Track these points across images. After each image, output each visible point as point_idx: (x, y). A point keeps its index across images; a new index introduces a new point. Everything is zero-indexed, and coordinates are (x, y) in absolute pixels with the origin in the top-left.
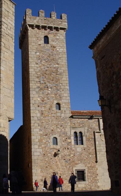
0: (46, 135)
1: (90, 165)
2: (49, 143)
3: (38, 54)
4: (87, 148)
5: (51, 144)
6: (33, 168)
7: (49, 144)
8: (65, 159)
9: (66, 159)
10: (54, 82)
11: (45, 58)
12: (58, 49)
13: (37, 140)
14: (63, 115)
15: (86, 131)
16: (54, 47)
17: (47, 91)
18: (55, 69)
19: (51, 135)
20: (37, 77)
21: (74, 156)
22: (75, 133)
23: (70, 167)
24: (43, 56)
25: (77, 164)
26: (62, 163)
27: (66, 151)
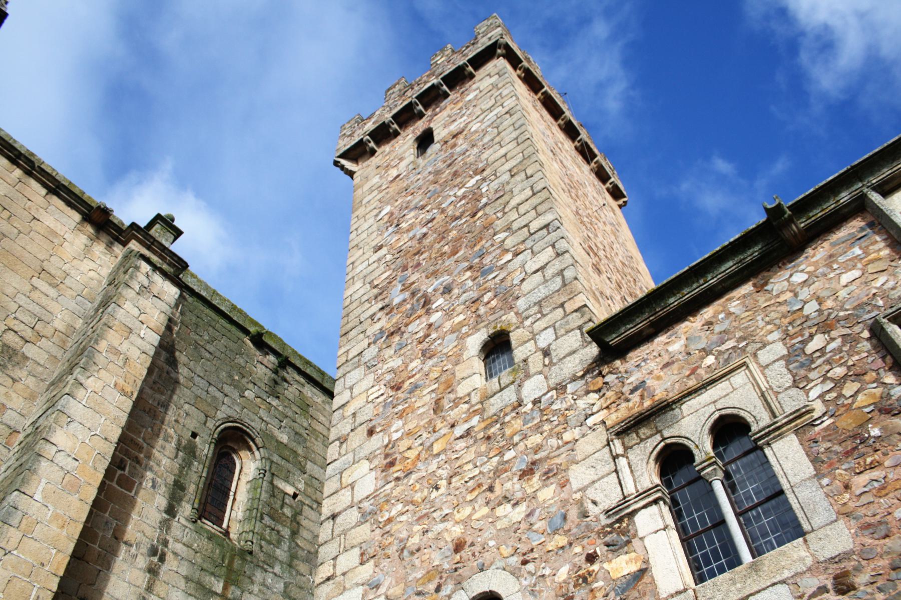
15: (780, 376)
22: (674, 459)
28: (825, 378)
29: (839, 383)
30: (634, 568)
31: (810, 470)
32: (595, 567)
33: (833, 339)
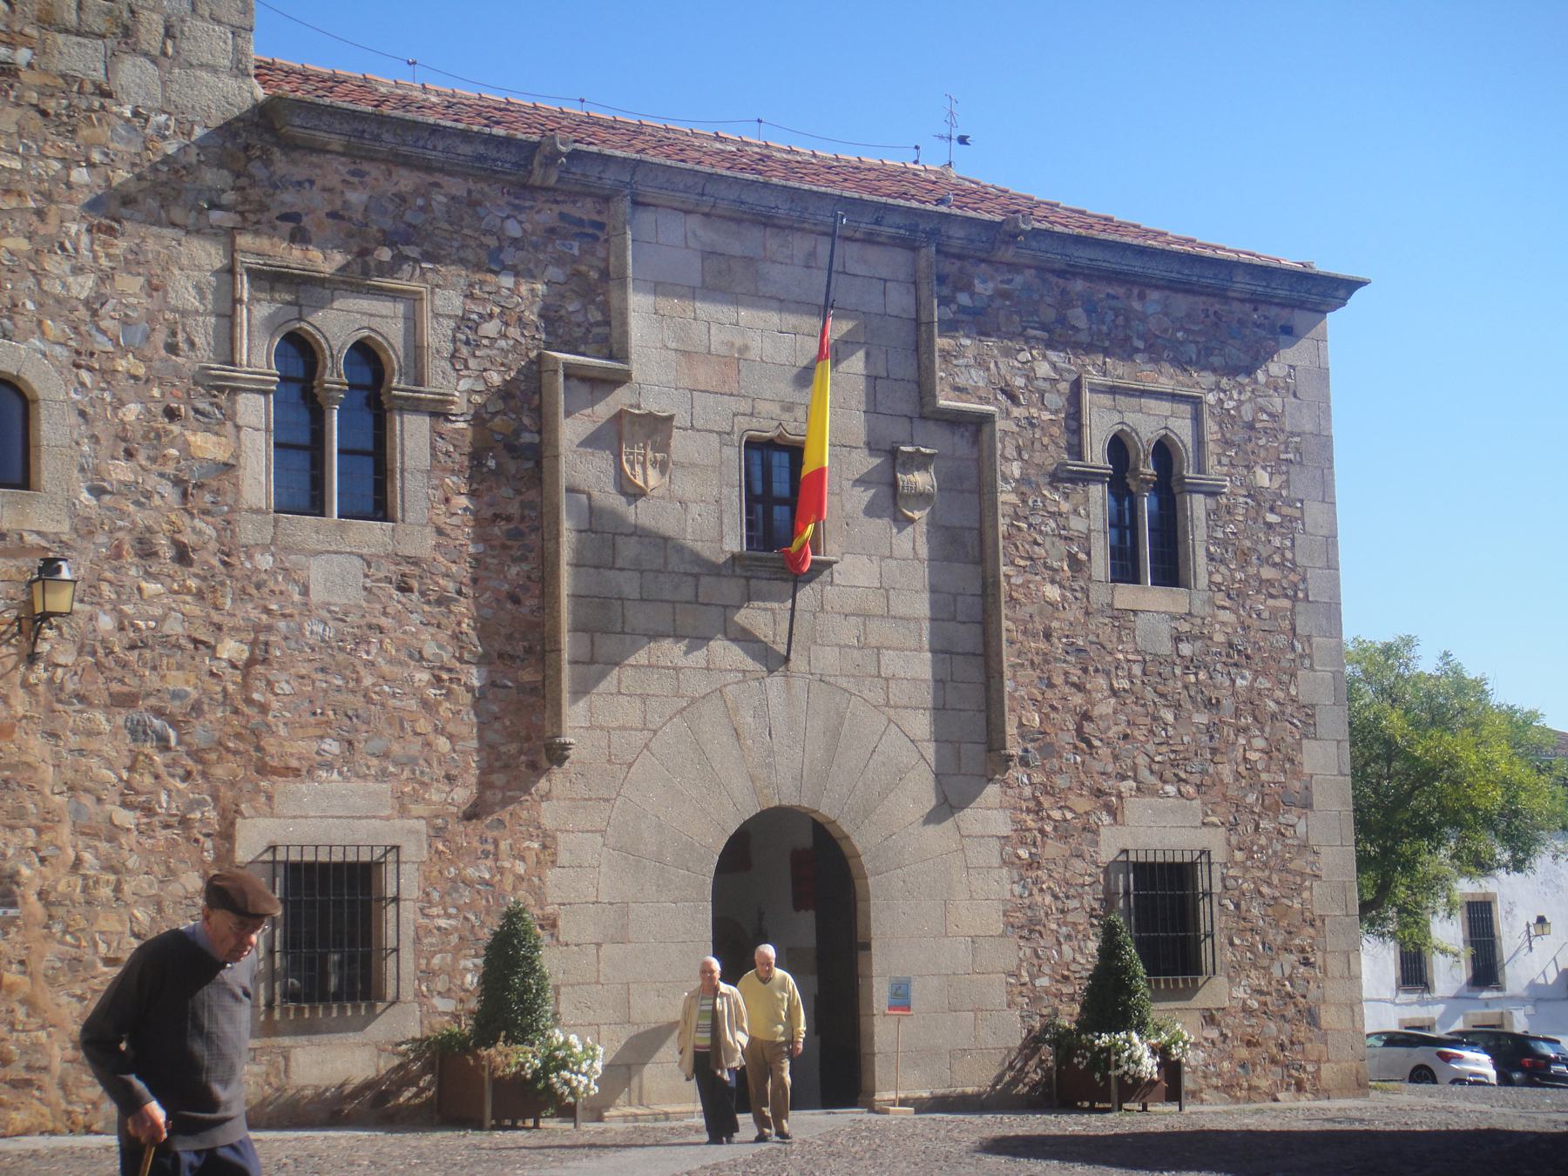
8: (125, 700)
14: (134, 76)
25: (296, 773)
27: (151, 588)
30: (222, 455)
31: (426, 461)
32: (175, 428)
33: (505, 336)
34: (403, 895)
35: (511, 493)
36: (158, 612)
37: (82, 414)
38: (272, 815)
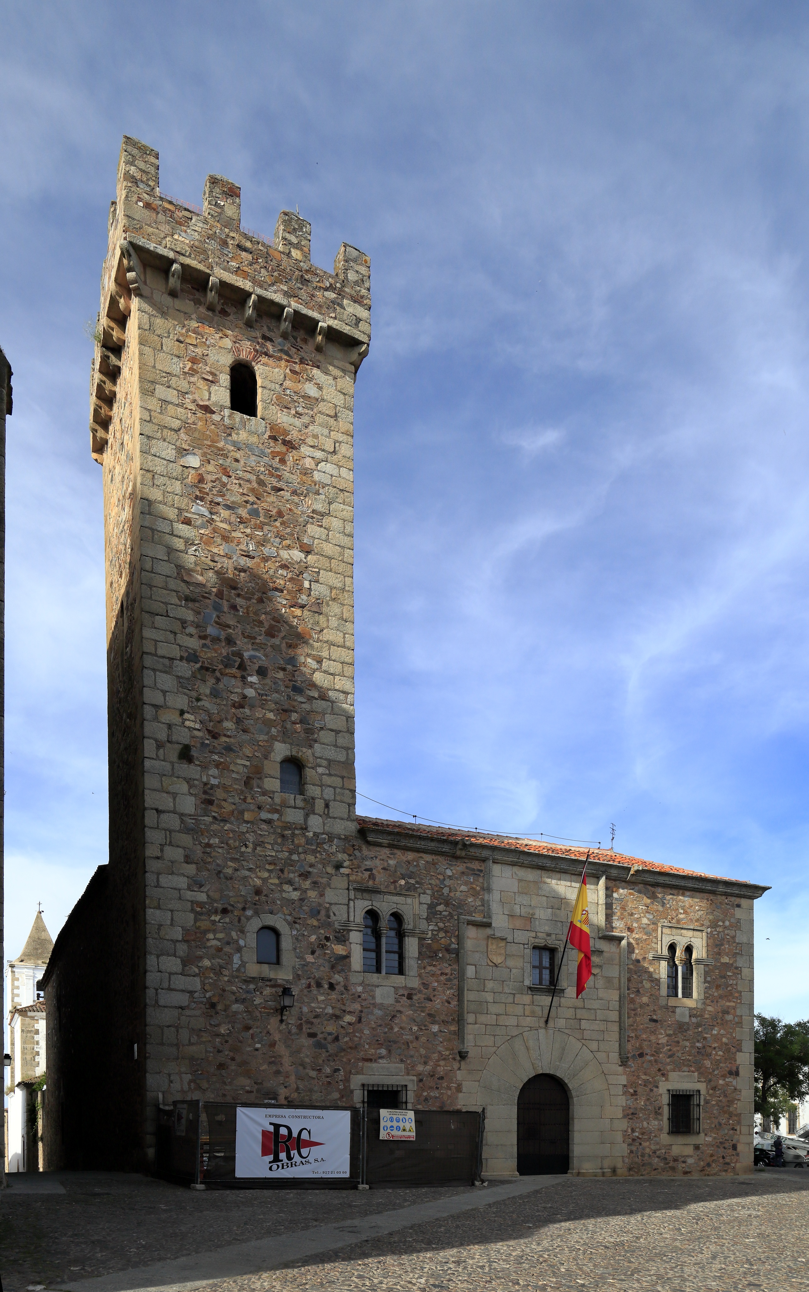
0: (225, 911)
1: (428, 1068)
2: (239, 950)
3: (194, 461)
4: (420, 992)
5: (250, 956)
6: (150, 1065)
7: (236, 959)
9: (320, 1036)
10: (276, 641)
11: (238, 499)
12: (308, 463)
13: (177, 933)
16: (285, 442)
17: (240, 684)
18: (284, 572)
19: (249, 913)
20: (187, 599)
21: (360, 1020)
23: (337, 1070)
24: (224, 485)
26: (299, 1051)
28: (436, 925)
29: (440, 929)
31: (417, 956)
32: (328, 944)
34: (409, 1101)
35: (447, 965)
36: (323, 1006)
37: (297, 939)
38: (363, 1074)
